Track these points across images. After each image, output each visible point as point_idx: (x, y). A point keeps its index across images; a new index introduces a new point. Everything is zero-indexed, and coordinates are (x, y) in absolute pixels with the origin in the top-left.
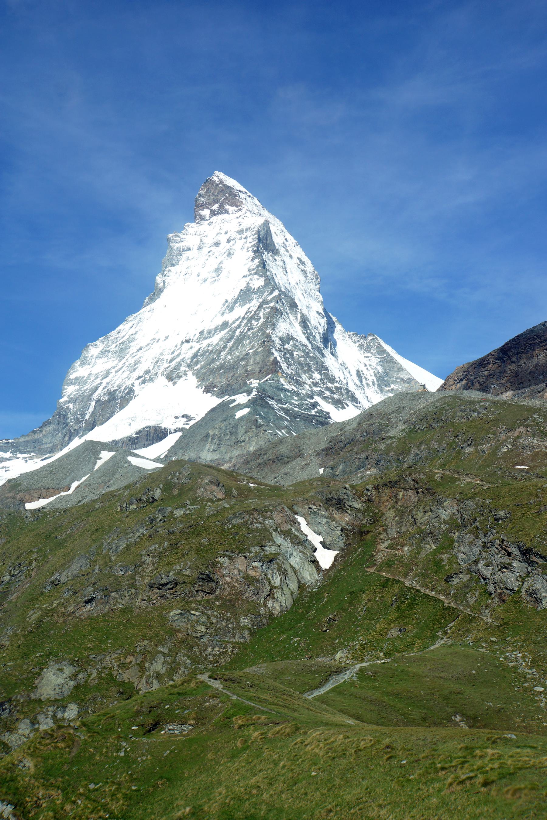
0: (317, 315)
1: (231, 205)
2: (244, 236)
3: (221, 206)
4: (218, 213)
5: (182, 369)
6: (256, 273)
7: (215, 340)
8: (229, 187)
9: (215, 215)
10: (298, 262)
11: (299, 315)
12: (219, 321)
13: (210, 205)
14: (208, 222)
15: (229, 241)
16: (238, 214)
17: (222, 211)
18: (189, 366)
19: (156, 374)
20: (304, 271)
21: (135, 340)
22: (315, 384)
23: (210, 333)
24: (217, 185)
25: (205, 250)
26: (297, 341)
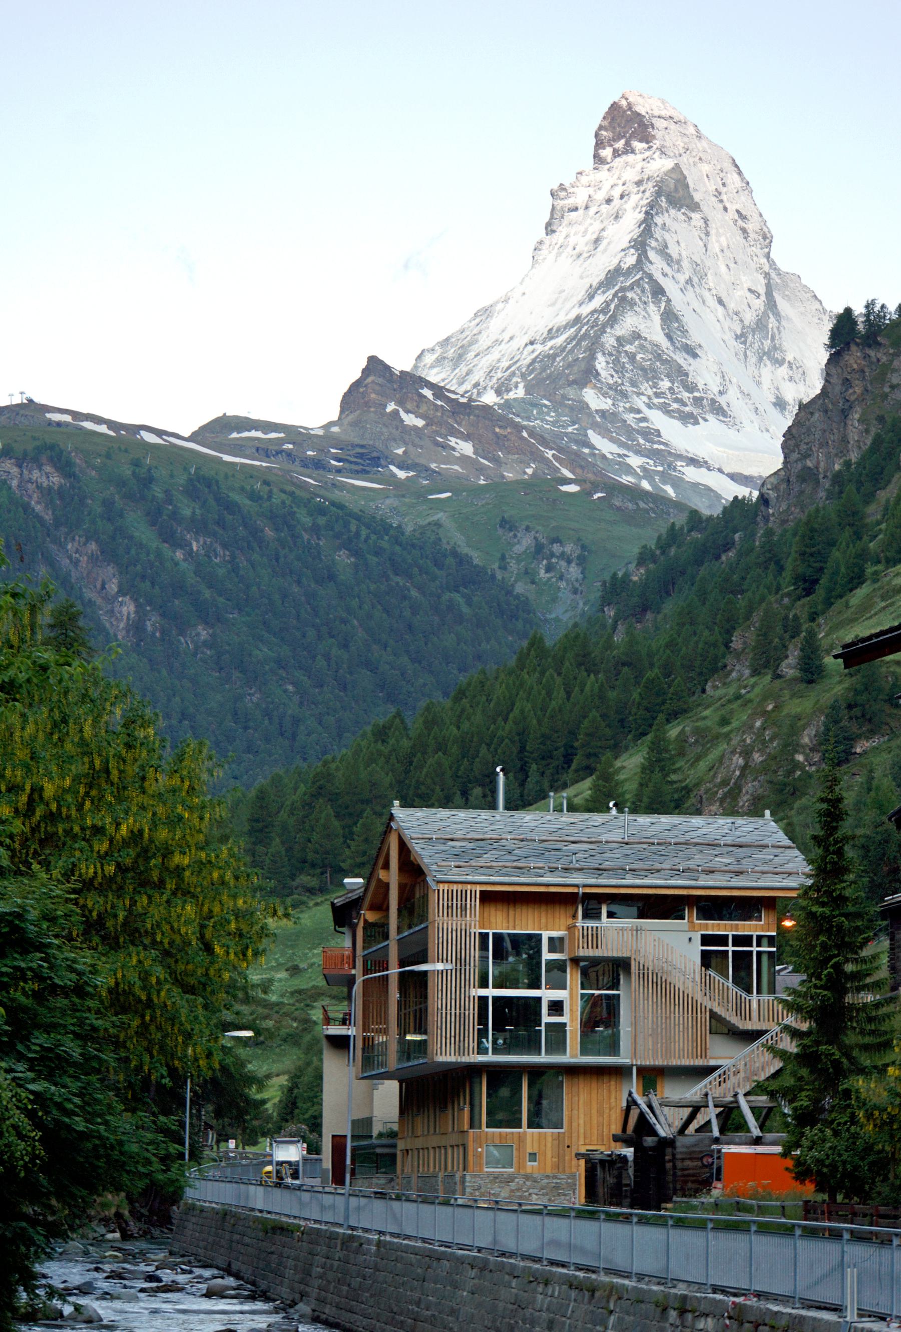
0: (749, 294)
1: (641, 141)
2: (642, 188)
3: (627, 144)
4: (623, 153)
5: (515, 380)
6: (632, 247)
7: (560, 341)
8: (639, 114)
9: (619, 155)
10: (736, 217)
11: (663, 304)
12: (572, 316)
13: (614, 140)
14: (607, 166)
15: (622, 197)
16: (648, 154)
17: (629, 150)
18: (523, 376)
19: (485, 388)
20: (744, 231)
21: (477, 341)
22: (657, 395)
23: (560, 330)
24: (625, 112)
25: (593, 210)
26: (646, 339)
